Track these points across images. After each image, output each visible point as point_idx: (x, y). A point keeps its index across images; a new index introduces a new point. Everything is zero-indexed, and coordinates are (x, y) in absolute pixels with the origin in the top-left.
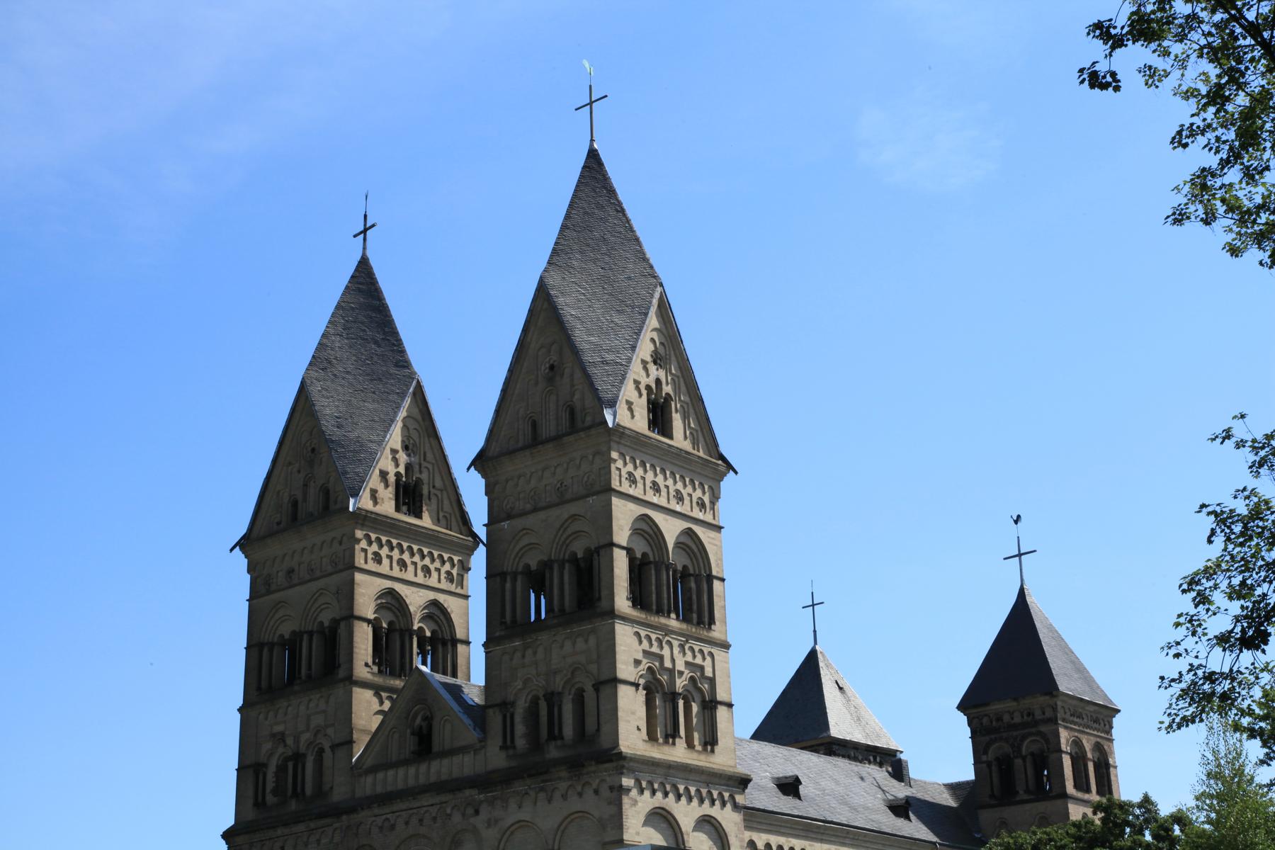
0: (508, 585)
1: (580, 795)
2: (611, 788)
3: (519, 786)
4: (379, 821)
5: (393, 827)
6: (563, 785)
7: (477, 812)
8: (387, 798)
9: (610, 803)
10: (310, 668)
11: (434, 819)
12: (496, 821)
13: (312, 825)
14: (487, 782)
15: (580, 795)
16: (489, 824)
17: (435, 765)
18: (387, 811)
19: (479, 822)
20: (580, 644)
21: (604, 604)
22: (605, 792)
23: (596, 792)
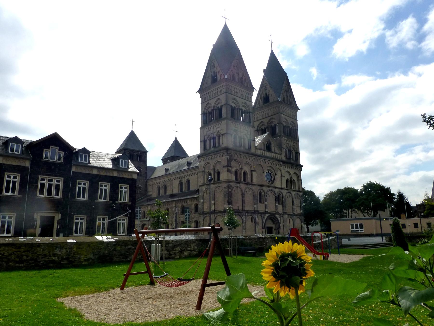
4: (263, 160)
8: (266, 157)
14: (283, 162)
16: (284, 169)
19: (282, 168)
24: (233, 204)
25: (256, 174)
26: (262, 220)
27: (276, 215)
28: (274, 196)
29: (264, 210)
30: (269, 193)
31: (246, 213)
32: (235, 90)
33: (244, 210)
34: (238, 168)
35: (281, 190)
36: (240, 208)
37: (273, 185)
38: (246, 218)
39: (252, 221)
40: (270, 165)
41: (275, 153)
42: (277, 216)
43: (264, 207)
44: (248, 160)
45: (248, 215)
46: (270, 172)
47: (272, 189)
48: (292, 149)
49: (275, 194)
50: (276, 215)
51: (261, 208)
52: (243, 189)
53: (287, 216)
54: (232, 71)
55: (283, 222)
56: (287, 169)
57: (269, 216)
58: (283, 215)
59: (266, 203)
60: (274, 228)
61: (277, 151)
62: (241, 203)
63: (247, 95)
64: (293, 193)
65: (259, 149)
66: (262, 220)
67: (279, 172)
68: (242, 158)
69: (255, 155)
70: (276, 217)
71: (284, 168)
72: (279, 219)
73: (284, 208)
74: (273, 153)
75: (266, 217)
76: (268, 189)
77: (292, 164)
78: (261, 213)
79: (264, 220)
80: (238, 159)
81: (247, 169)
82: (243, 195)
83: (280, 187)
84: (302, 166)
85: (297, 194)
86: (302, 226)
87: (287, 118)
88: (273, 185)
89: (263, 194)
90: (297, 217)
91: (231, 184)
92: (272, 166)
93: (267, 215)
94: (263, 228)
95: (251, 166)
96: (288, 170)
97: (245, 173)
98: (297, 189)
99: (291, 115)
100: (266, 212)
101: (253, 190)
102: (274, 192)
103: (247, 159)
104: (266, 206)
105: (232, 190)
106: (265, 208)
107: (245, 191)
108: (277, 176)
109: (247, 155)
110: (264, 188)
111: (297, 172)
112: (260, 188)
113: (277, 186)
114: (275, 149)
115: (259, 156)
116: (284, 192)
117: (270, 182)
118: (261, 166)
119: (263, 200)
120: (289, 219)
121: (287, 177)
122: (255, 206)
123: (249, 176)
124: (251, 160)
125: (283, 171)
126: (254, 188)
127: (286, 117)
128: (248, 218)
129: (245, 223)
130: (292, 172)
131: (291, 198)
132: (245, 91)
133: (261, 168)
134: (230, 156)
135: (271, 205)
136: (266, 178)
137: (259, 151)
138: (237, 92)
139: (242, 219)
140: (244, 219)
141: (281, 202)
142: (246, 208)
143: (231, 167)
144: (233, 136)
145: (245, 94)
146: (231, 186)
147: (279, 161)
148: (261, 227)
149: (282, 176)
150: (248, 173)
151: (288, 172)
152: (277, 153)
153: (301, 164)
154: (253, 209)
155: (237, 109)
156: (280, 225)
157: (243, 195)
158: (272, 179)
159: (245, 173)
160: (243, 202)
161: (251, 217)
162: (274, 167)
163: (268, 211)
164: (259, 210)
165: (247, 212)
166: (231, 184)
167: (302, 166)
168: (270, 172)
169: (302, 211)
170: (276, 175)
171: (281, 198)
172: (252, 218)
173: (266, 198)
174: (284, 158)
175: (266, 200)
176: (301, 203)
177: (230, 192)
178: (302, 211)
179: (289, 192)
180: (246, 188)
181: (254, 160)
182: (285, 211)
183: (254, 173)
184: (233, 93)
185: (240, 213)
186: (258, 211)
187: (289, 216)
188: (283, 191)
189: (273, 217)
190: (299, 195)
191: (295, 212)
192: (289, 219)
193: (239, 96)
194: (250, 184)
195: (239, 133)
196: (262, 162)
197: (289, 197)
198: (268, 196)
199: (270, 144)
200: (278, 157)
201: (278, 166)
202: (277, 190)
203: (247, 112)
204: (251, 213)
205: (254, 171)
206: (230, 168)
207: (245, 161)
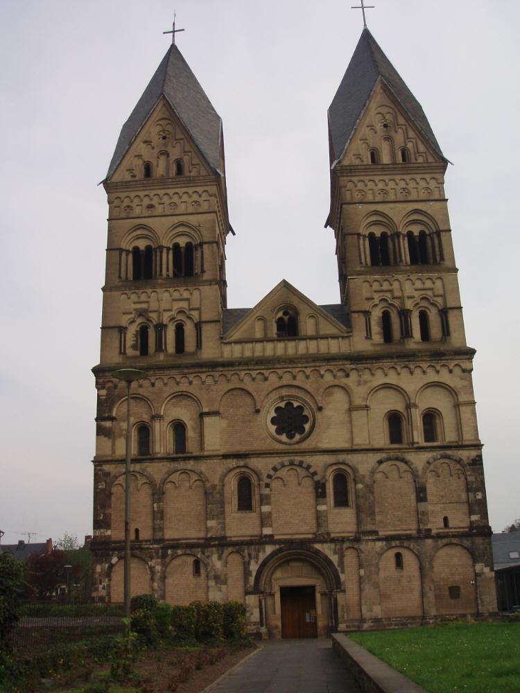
0: (361, 242)
1: (438, 372)
2: (464, 371)
3: (387, 364)
4: (254, 373)
5: (266, 379)
6: (424, 365)
7: (348, 376)
9: (462, 379)
10: (168, 270)
11: (308, 377)
12: (365, 382)
13: (186, 371)
14: (357, 359)
15: (438, 372)
16: (359, 383)
17: (291, 345)
18: (263, 367)
19: (351, 381)
20: (428, 284)
21: (447, 263)
22: (457, 371)
23: (451, 371)
24: (113, 526)
25: (224, 423)
26: (246, 565)
27: (318, 546)
28: (308, 483)
29: (257, 532)
30: (283, 473)
31: (165, 548)
32: (146, 201)
33: (162, 540)
34: (146, 418)
35: (341, 457)
36: (145, 534)
37: (304, 446)
38: (165, 565)
39: (197, 571)
40: (287, 379)
41: (315, 338)
42: (327, 549)
43: (257, 522)
44: (184, 387)
45: (175, 557)
46: (296, 404)
47: (297, 459)
48: (409, 305)
49: (315, 473)
50: (318, 546)
51: (240, 525)
52: (158, 478)
53: (379, 544)
54: (139, 156)
55: (360, 566)
56: (379, 379)
57: (280, 550)
58: (357, 540)
59: (265, 509)
60: (318, 589)
61: (330, 330)
62: (149, 522)
63: (195, 197)
64: (419, 460)
65: (236, 343)
66: (246, 565)
67: (339, 396)
68: (159, 384)
69: (213, 365)
70: (317, 552)
71: (366, 376)
72: (335, 559)
73: (363, 516)
74: (305, 338)
75: (262, 556)
76: (276, 461)
77: (408, 358)
78: (239, 546)
79: (254, 567)
80: (141, 391)
81: (184, 413)
82: (158, 494)
83: (346, 445)
84: (472, 352)
85: (448, 457)
86: (477, 575)
87: (379, 208)
88: (304, 446)
89: (254, 480)
90: (445, 541)
91: (107, 468)
92: (295, 383)
93: (269, 549)
94: (247, 593)
95: (197, 401)
96: (392, 379)
97: (179, 427)
98: (450, 436)
99: (409, 193)
100: (263, 540)
101: (200, 474)
102: (309, 467)
103: (178, 383)
104: (265, 520)
105: (109, 485)
106: (262, 525)
107: (164, 482)
108: (327, 412)
109: (173, 372)
110: (255, 463)
111: (444, 377)
112: (232, 463)
113: (325, 445)
114: (317, 324)
115: (230, 364)
116: (364, 464)
117: (297, 437)
118: (249, 393)
119: (256, 499)
120: (398, 557)
121: (388, 403)
122: (211, 523)
123: (191, 433)
124: (196, 382)
125: (359, 394)
126: (203, 467)
127: (379, 208)
128: (177, 562)
129: (164, 578)
130: (411, 382)
131: (408, 476)
132: (181, 191)
133: (248, 400)
134: (109, 389)
135: (292, 511)
136: (273, 428)
137: (237, 348)
138: (151, 207)
139: (151, 568)
140: (158, 568)
141: (351, 497)
142: (169, 534)
143: (112, 419)
144: (132, 330)
145: (185, 198)
146: (108, 474)
147: (329, 359)
148: (241, 590)
149: (351, 409)
150: (189, 424)
151: (387, 386)
152: (325, 337)
153: (470, 344)
154: (202, 535)
155: (155, 249)
156: (338, 578)
157: (158, 494)
158: (307, 427)
159: (179, 427)
160: (158, 515)
161: (191, 560)
162: (308, 387)
163: (271, 536)
164: (229, 534)
165: (175, 545)
166: (107, 468)
167: (473, 352)
168: (296, 404)
169: (474, 518)
170: (320, 409)
171: (351, 485)
172: (197, 564)
173: (266, 491)
174: (359, 343)
175: (264, 500)
176: (468, 490)
177: (103, 491)
178: (474, 518)
179: (388, 459)
180: (170, 474)
181: (209, 381)
182: (369, 528)
183: (207, 420)
184: (137, 211)
185: (141, 549)
186: (224, 538)
187: (393, 544)
188: (353, 459)
189: (296, 551)
190: (459, 461)
191: (436, 525)
192: (398, 557)
193: (159, 210)
194: (197, 458)
195: (153, 316)
196: (247, 379)
197: (395, 475)
198: (275, 484)
199: (297, 313)
200: (334, 347)
201: (328, 378)
202: (318, 462)
203: (196, 247)
204: (190, 546)
205: (208, 414)
206: (108, 424)
207: (172, 388)
